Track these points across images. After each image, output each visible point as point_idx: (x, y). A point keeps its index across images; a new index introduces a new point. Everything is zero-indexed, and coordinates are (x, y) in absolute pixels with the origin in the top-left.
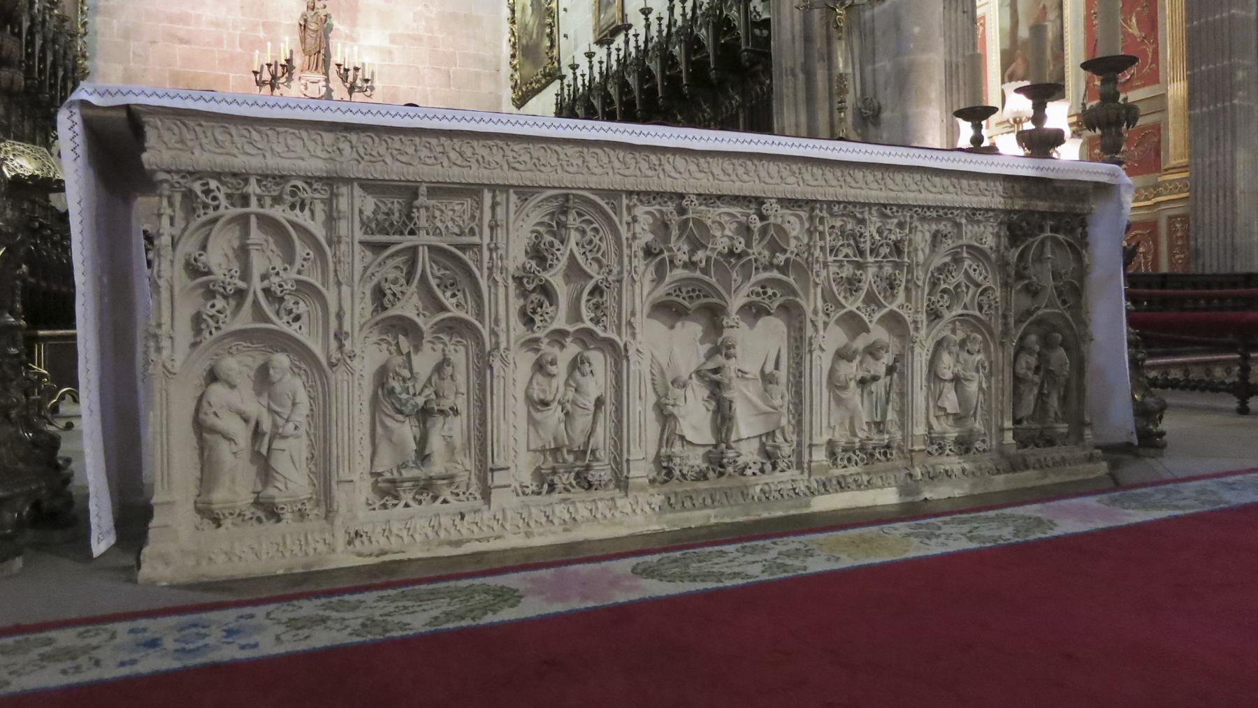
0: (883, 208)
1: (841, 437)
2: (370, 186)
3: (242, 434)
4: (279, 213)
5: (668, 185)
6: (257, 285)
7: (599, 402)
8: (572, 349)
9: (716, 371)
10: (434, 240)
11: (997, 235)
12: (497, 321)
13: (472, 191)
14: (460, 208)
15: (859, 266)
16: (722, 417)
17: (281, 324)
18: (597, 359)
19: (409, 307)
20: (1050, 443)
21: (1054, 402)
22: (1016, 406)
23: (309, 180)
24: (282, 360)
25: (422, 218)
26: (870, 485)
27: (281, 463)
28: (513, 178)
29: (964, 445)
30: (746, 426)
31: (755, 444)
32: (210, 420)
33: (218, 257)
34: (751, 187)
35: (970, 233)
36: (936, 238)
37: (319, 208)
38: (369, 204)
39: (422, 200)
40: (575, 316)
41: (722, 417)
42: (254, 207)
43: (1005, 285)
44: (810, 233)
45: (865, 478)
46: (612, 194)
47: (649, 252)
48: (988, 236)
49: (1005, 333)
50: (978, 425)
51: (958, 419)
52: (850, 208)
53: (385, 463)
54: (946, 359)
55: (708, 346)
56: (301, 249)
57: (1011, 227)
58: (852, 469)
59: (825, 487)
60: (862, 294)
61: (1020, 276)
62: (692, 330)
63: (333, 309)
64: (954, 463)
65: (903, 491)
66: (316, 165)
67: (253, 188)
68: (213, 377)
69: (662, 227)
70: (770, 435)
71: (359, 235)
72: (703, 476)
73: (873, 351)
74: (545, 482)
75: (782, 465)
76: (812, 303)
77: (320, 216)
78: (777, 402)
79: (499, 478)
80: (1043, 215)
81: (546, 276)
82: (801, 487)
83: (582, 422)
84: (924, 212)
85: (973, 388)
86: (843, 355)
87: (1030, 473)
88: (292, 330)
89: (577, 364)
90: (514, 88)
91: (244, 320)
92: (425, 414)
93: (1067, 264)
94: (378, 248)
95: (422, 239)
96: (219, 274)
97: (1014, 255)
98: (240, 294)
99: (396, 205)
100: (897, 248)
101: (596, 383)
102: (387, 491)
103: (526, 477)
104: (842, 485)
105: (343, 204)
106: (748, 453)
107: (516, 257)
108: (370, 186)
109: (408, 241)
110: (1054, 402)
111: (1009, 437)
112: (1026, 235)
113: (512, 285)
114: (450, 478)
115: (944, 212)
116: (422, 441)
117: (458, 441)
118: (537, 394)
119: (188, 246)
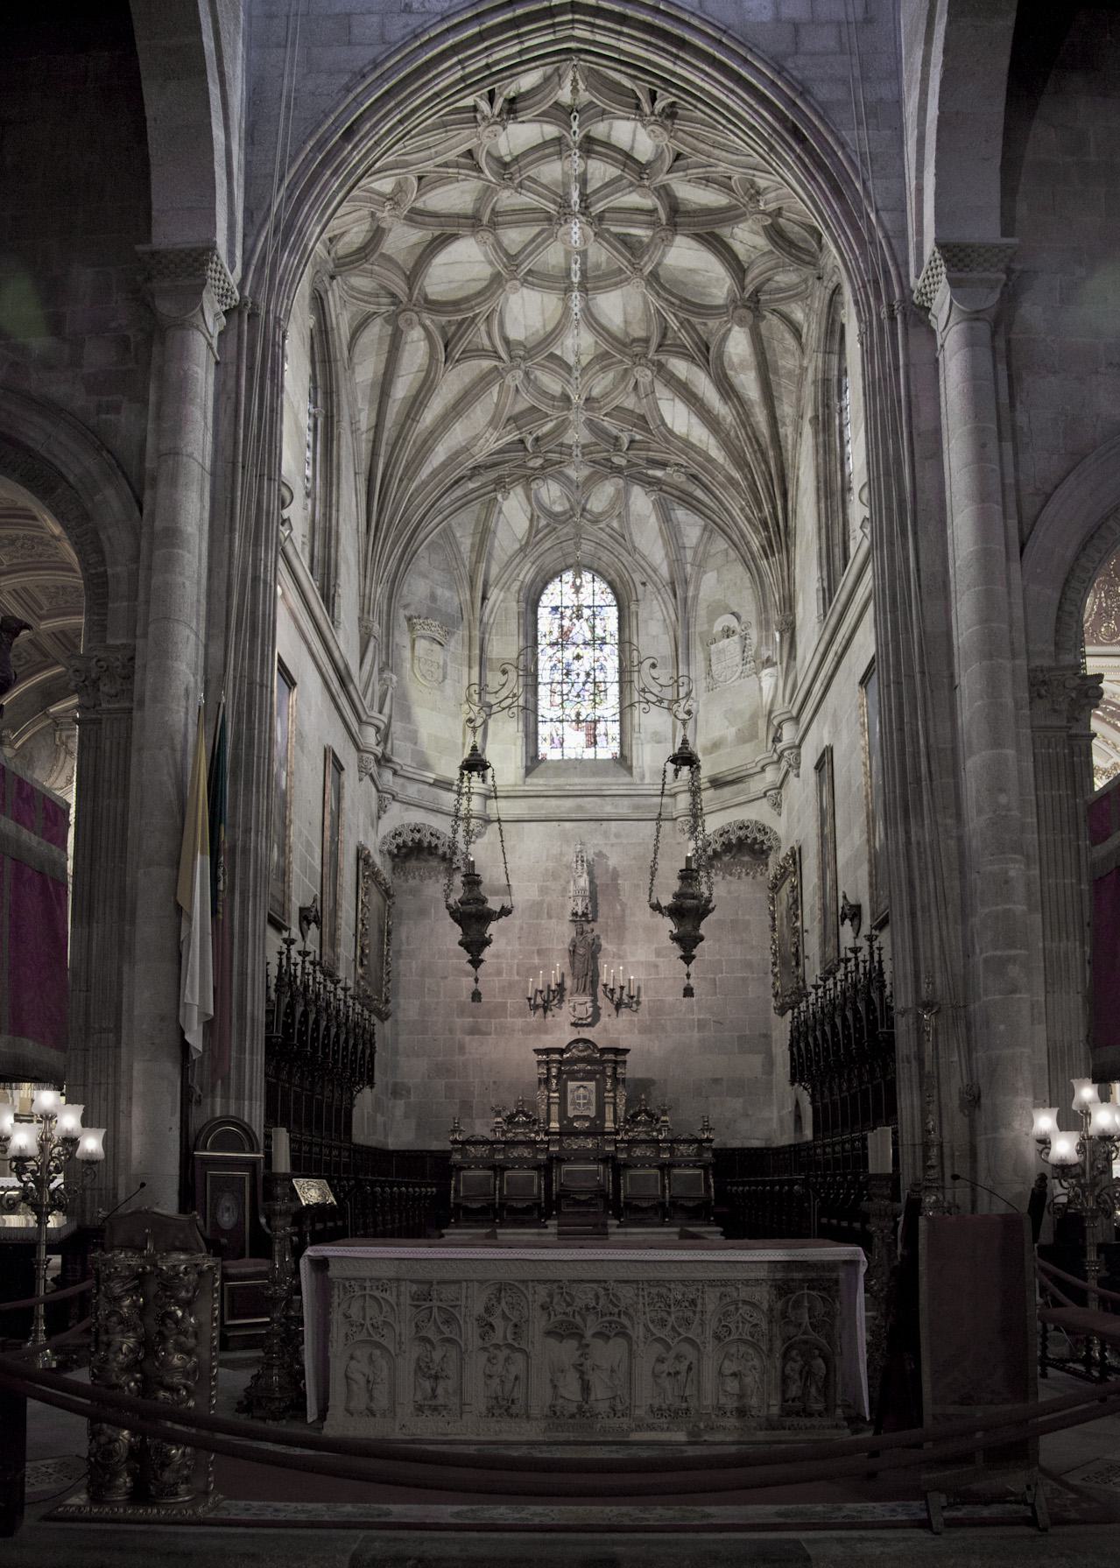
0: (682, 1282)
1: (657, 1403)
2: (412, 1281)
3: (362, 1381)
4: (377, 1293)
5: (550, 1276)
6: (368, 1322)
7: (516, 1378)
8: (506, 1352)
9: (581, 1365)
10: (439, 1304)
11: (768, 1292)
12: (467, 1340)
13: (458, 1282)
14: (454, 1288)
15: (669, 1313)
16: (586, 1388)
17: (376, 1338)
18: (518, 1356)
19: (431, 1333)
20: (811, 1415)
21: (813, 1390)
22: (784, 1392)
23: (389, 1280)
24: (377, 1352)
25: (434, 1294)
26: (668, 1429)
27: (376, 1394)
28: (474, 1276)
29: (742, 1412)
30: (599, 1392)
31: (607, 1404)
32: (350, 1375)
33: (355, 1312)
34: (601, 1275)
35: (744, 1293)
36: (723, 1296)
37: (394, 1289)
38: (414, 1288)
39: (435, 1287)
40: (505, 1338)
41: (586, 1388)
42: (368, 1292)
43: (770, 1322)
44: (637, 1295)
45: (665, 1426)
46: (523, 1281)
47: (543, 1307)
48: (763, 1295)
49: (771, 1350)
50: (754, 1401)
51: (741, 1397)
52: (659, 1283)
53: (419, 1397)
54: (727, 1363)
55: (579, 1353)
56: (386, 1308)
57: (778, 1288)
58: (664, 1420)
59: (639, 1428)
60: (669, 1327)
61: (784, 1315)
62: (574, 1343)
63: (397, 1332)
64: (732, 1422)
65: (689, 1434)
66: (392, 1274)
67: (368, 1284)
68: (352, 1358)
69: (551, 1296)
70: (614, 1398)
71: (409, 1301)
72: (572, 1416)
73: (679, 1357)
74: (490, 1412)
75: (619, 1414)
76: (638, 1332)
77: (394, 1293)
78: (616, 1382)
79: (467, 1408)
80: (803, 1280)
81: (490, 1319)
82: (625, 1427)
83: (508, 1386)
84: (712, 1283)
85: (748, 1380)
86: (661, 1360)
87: (787, 1432)
88: (381, 1340)
89: (507, 1359)
90: (776, 995)
91: (363, 1336)
92: (436, 1378)
93: (820, 1308)
94: (417, 1307)
95: (435, 1303)
96: (354, 1318)
97: (779, 1305)
98: (362, 1325)
99: (426, 1287)
100: (693, 1302)
101: (518, 1367)
102: (420, 1409)
103: (483, 1409)
104: (651, 1428)
105: (403, 1289)
106: (603, 1407)
107: (478, 1309)
108: (412, 1281)
109: (428, 1304)
110: (813, 1390)
111: (775, 1410)
112: (787, 1293)
113: (475, 1323)
114: (445, 1406)
115: (725, 1283)
116: (433, 1390)
117: (451, 1391)
118: (488, 1372)
119: (344, 1306)
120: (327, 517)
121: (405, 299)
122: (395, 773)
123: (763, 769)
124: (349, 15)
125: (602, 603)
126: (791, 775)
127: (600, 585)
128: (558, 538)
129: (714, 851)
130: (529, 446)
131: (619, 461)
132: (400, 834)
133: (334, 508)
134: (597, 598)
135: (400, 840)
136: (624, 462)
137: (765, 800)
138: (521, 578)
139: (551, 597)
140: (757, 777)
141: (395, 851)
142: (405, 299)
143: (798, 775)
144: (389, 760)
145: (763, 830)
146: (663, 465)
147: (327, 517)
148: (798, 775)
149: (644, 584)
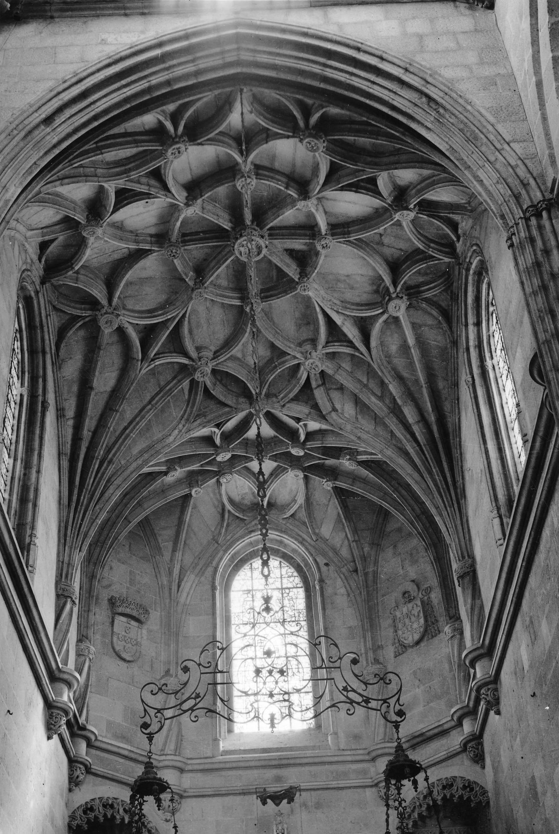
120: (26, 475)
121: (104, 302)
122: (90, 745)
123: (460, 724)
124: (56, 47)
125: (290, 585)
126: (492, 713)
127: (288, 570)
128: (247, 529)
129: (420, 815)
130: (218, 441)
131: (297, 452)
132: (92, 809)
133: (34, 471)
134: (285, 581)
135: (91, 815)
136: (302, 453)
137: (464, 755)
138: (214, 563)
139: (242, 582)
140: (454, 733)
141: (86, 827)
142: (104, 302)
143: (498, 713)
144: (84, 728)
145: (469, 786)
146: (336, 452)
147: (26, 475)
148: (498, 713)
149: (327, 565)
